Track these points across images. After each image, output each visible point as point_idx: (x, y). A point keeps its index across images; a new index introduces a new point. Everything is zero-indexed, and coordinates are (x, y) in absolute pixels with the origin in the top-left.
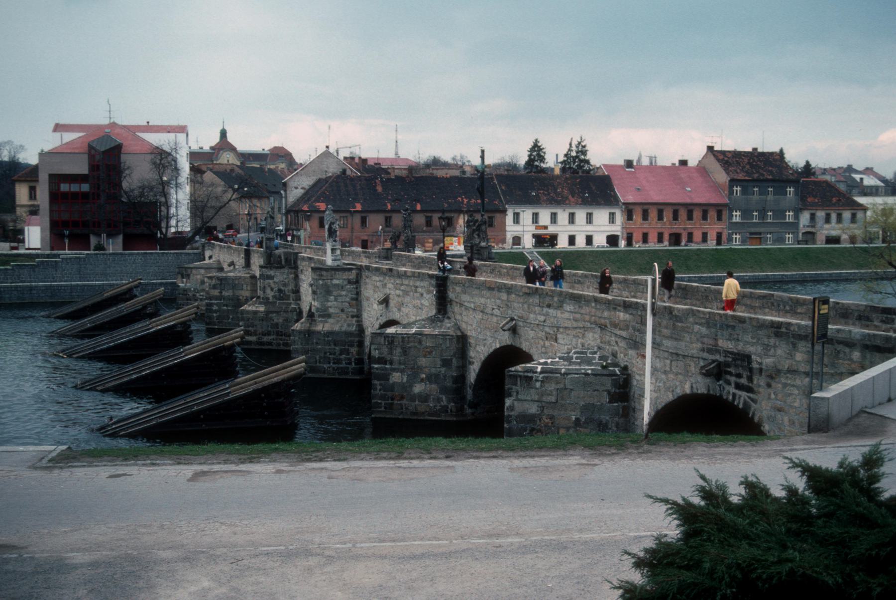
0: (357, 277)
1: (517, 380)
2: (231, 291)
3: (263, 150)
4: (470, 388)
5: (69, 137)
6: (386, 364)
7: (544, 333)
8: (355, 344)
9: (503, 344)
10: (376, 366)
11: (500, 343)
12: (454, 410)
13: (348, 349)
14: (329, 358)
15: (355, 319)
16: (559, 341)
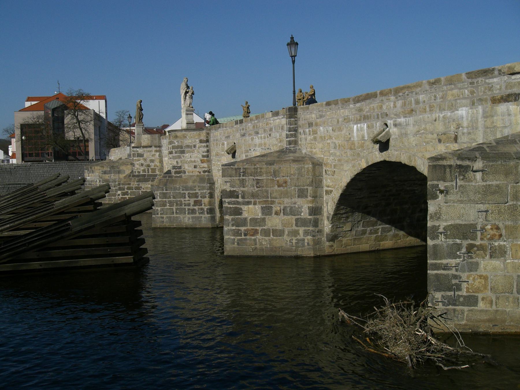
0: (207, 137)
1: (445, 173)
2: (117, 175)
3: (158, 127)
4: (328, 218)
5: (34, 103)
6: (238, 197)
7: (435, 136)
8: (207, 196)
9: (370, 164)
10: (227, 200)
11: (367, 162)
12: (311, 243)
13: (201, 200)
14: (185, 209)
15: (207, 173)
16: (459, 140)
